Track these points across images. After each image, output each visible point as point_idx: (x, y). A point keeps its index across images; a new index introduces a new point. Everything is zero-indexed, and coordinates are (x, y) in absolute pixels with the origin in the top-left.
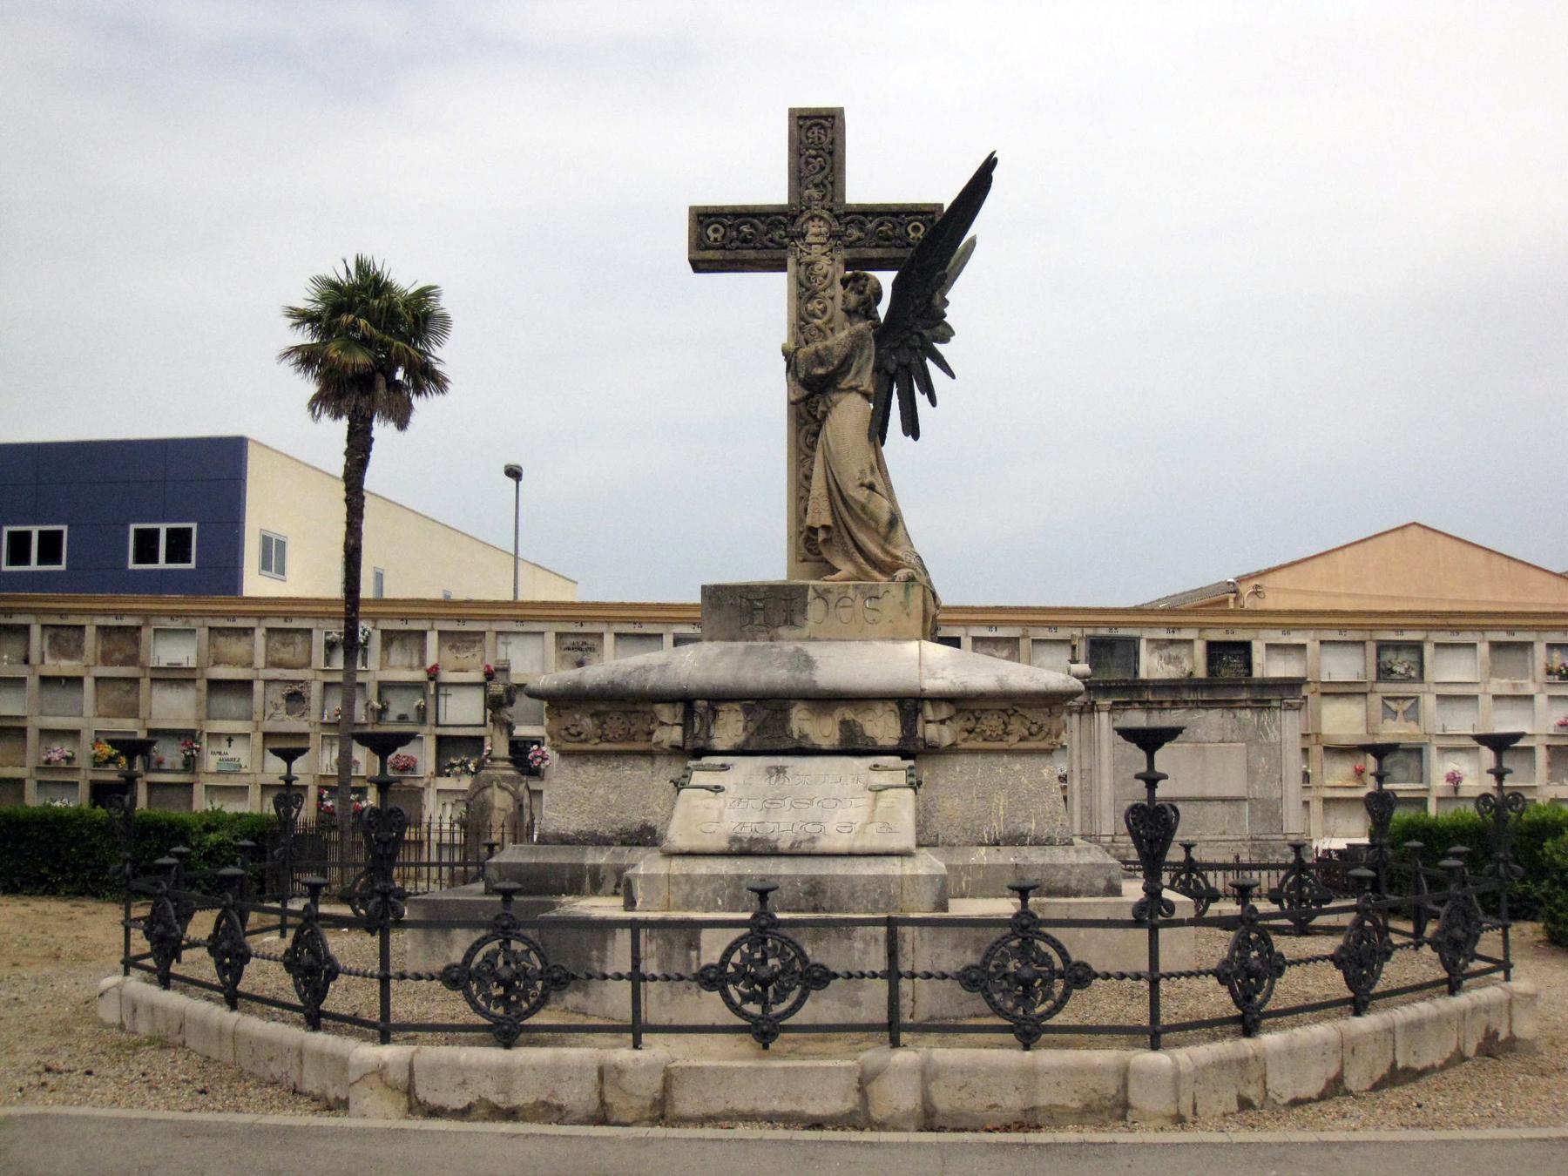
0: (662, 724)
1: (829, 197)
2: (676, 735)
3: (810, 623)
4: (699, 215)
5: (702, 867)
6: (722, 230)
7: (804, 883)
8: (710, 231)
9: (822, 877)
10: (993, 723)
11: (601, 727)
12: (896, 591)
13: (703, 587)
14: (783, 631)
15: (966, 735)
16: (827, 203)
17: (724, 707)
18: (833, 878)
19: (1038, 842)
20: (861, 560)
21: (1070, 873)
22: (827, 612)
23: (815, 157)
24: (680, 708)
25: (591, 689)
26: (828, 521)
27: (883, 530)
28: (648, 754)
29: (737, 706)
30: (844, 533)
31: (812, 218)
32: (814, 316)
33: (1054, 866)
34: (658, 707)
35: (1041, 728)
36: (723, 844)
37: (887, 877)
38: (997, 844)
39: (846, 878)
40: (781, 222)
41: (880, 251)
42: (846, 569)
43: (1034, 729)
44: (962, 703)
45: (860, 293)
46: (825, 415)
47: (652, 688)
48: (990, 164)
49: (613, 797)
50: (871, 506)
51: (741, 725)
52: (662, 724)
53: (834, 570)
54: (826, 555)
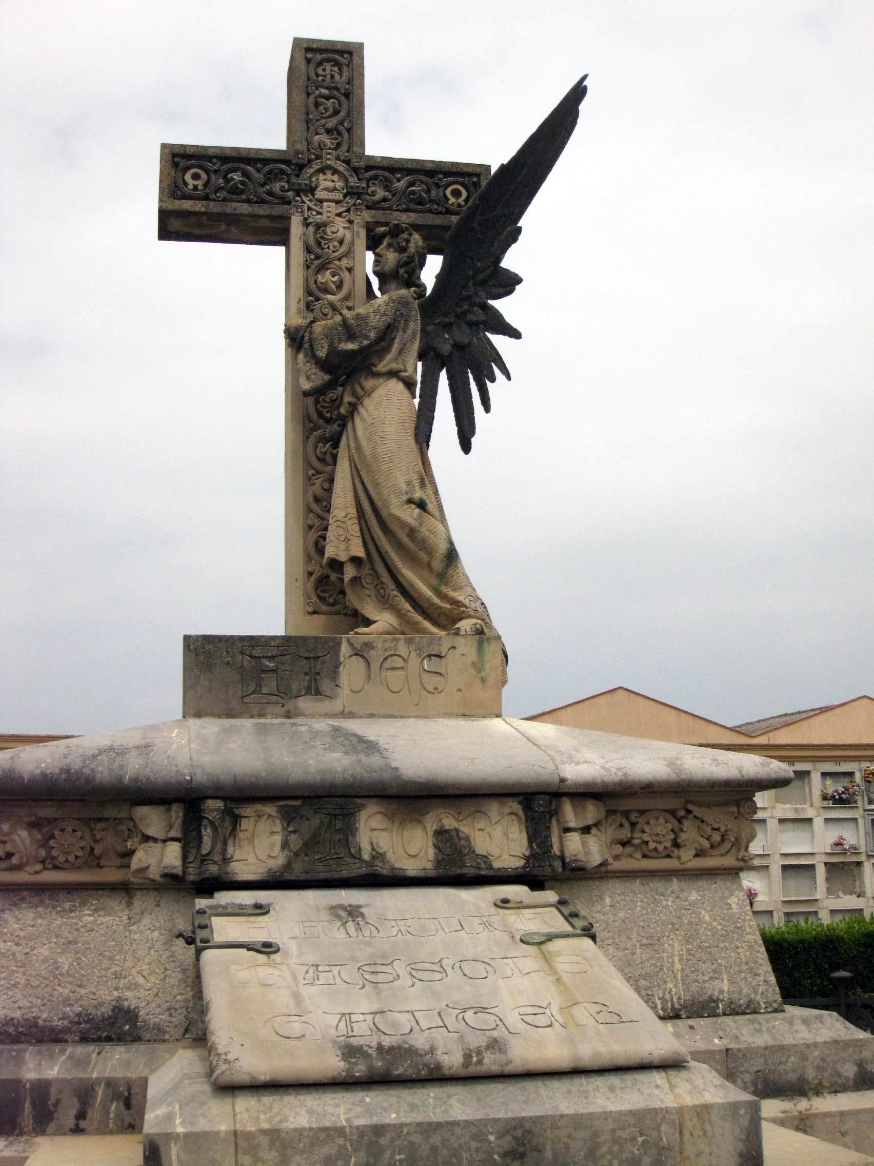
0: (147, 838)
1: (344, 147)
2: (172, 856)
3: (344, 692)
4: (174, 155)
5: (299, 1113)
6: (204, 176)
7: (500, 1136)
8: (188, 177)
9: (536, 1120)
10: (659, 830)
11: (44, 844)
12: (466, 648)
13: (187, 638)
14: (305, 703)
15: (619, 849)
16: (342, 152)
17: (248, 811)
18: (555, 1121)
19: (734, 1010)
20: (407, 606)
21: (804, 1058)
22: (368, 677)
23: (327, 98)
24: (177, 813)
25: (33, 780)
26: (360, 552)
27: (437, 565)
28: (124, 889)
29: (270, 809)
30: (373, 573)
31: (322, 171)
32: (327, 291)
33: (782, 1048)
34: (142, 811)
35: (723, 838)
36: (333, 1064)
37: (655, 1111)
38: (677, 1016)
39: (577, 1121)
40: (282, 172)
41: (412, 215)
42: (384, 620)
43: (717, 837)
44: (615, 800)
45: (402, 250)
46: (353, 408)
47: (135, 780)
48: (578, 93)
49: (65, 961)
50: (424, 531)
51: (278, 839)
52: (147, 838)
53: (368, 622)
54: (353, 599)
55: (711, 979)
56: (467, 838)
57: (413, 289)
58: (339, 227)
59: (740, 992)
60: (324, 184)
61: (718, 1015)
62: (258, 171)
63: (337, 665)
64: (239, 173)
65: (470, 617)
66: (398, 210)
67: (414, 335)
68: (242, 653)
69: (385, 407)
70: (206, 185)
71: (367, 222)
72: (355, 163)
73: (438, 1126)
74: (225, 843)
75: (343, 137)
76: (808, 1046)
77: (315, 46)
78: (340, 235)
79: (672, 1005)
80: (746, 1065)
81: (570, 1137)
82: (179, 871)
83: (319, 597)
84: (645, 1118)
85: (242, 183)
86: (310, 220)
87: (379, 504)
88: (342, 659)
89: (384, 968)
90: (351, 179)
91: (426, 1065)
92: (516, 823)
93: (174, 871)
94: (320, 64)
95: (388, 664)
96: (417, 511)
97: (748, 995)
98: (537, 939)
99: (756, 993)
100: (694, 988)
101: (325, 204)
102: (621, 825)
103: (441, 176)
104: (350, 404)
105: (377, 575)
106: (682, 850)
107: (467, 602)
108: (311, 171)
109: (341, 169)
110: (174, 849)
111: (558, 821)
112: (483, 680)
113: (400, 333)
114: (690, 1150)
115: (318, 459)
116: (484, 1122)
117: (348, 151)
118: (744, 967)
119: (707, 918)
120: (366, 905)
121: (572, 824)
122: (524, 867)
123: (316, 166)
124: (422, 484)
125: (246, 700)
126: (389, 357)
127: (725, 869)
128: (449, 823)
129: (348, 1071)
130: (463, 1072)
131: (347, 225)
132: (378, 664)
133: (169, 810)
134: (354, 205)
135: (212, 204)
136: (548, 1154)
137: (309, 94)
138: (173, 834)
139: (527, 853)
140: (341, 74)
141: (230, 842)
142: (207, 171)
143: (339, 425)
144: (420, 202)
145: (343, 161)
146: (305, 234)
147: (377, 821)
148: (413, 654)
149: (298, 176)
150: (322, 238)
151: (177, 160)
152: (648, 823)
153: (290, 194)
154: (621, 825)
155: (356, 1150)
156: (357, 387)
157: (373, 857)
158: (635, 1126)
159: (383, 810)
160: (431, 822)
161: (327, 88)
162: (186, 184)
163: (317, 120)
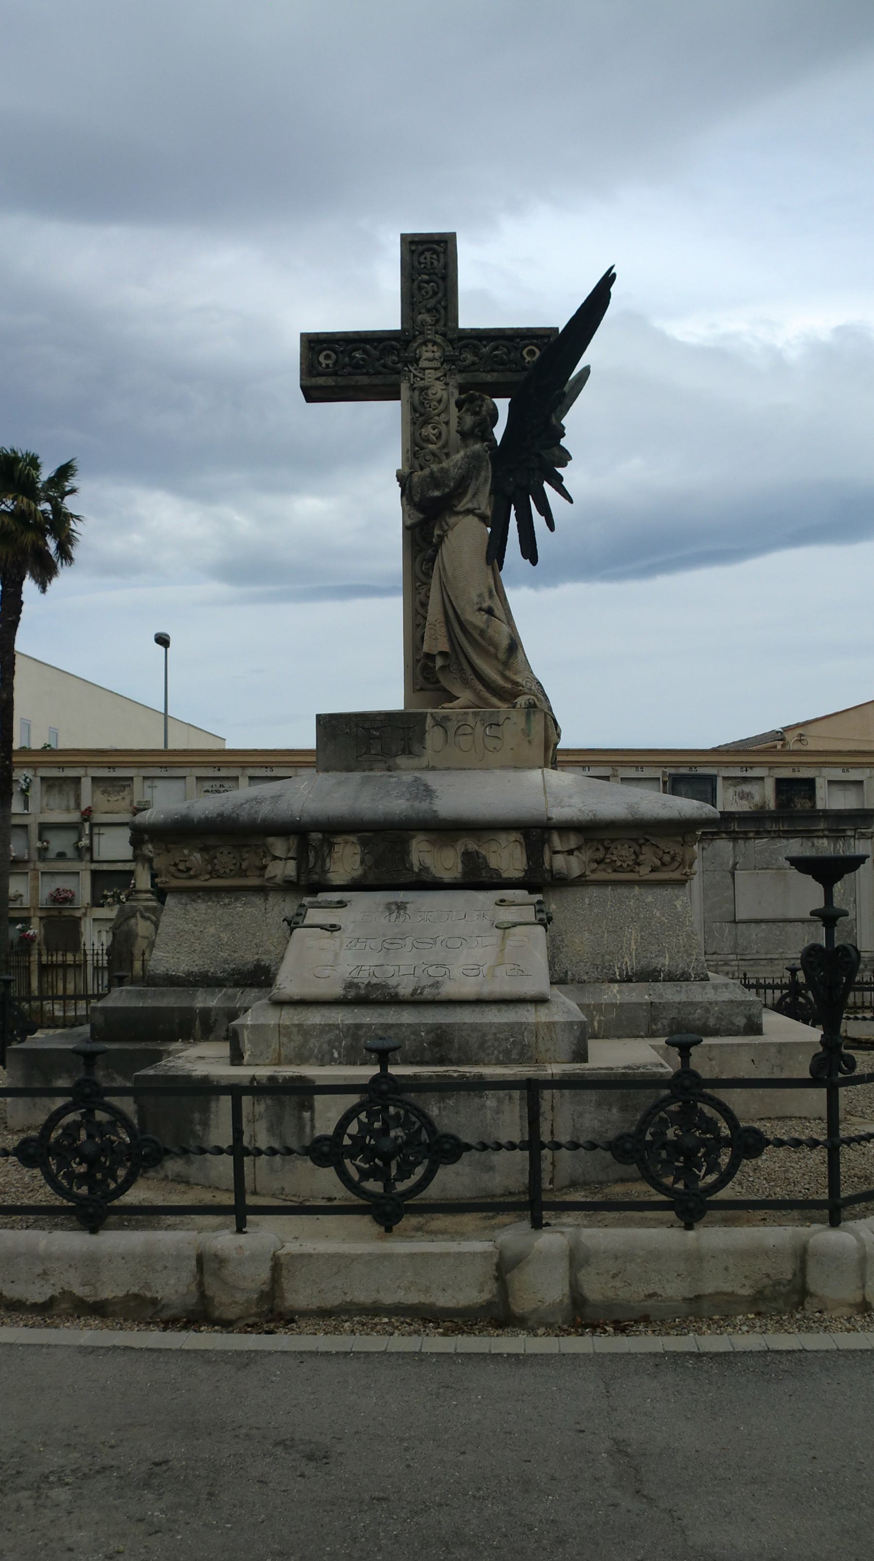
0: (275, 858)
1: (442, 323)
2: (289, 869)
3: (429, 752)
4: (310, 342)
5: (315, 1017)
6: (333, 356)
7: (428, 1033)
8: (321, 358)
9: (449, 1025)
10: (624, 853)
11: (211, 861)
12: (517, 718)
13: (318, 716)
14: (401, 761)
15: (595, 865)
16: (440, 328)
17: (339, 839)
18: (461, 1026)
19: (671, 978)
20: (480, 687)
21: (707, 1010)
22: (446, 741)
23: (428, 282)
24: (293, 841)
25: (200, 821)
26: (446, 648)
27: (502, 656)
28: (262, 891)
29: (353, 838)
31: (425, 343)
32: (428, 440)
33: (691, 1003)
34: (271, 840)
35: (673, 858)
36: (338, 991)
37: (522, 1024)
38: (630, 980)
39: (474, 1027)
40: (393, 348)
41: (495, 374)
42: (465, 696)
43: (667, 858)
44: (591, 832)
45: (476, 414)
46: (441, 538)
47: (264, 820)
48: (608, 279)
49: (225, 936)
50: (490, 632)
51: (358, 858)
52: (275, 858)
53: (453, 698)
54: (444, 683)
55: (657, 956)
56: (484, 858)
57: (486, 443)
58: (438, 390)
59: (677, 966)
60: (426, 355)
61: (660, 981)
62: (375, 348)
63: (424, 732)
64: (361, 352)
65: (525, 693)
66: (484, 371)
67: (486, 480)
68: (357, 726)
69: (465, 536)
70: (335, 364)
71: (459, 384)
72: (450, 336)
73: (392, 1025)
74: (324, 861)
75: (440, 314)
76: (711, 1003)
77: (417, 239)
78: (438, 396)
79: (627, 973)
80: (665, 1014)
81: (469, 1035)
82: (294, 879)
83: (425, 678)
84: (516, 1028)
85: (363, 359)
86: (415, 386)
87: (459, 612)
88: (427, 728)
89: (400, 941)
90: (447, 349)
91: (389, 994)
92: (519, 847)
93: (291, 879)
94: (422, 253)
95: (460, 732)
96: (486, 616)
97: (683, 968)
98: (506, 925)
99: (689, 967)
100: (643, 962)
101: (427, 371)
102: (598, 849)
103: (518, 340)
104: (438, 535)
105: (460, 664)
106: (642, 867)
107: (524, 683)
108: (416, 345)
109: (439, 341)
110: (292, 864)
111: (550, 847)
112: (530, 742)
113: (474, 481)
114: (542, 1048)
115: (423, 573)
116: (419, 1025)
117: (445, 325)
118: (682, 949)
119: (658, 914)
120: (412, 902)
121: (559, 848)
122: (524, 877)
123: (420, 341)
124: (491, 595)
125: (360, 759)
126: (465, 500)
127: (673, 881)
128: (472, 846)
129: (344, 995)
130: (412, 999)
131: (444, 387)
132: (453, 732)
133: (288, 839)
134: (450, 370)
135: (339, 379)
136: (456, 1045)
137: (413, 281)
138: (290, 855)
139: (526, 868)
140: (438, 261)
141: (328, 860)
142: (336, 352)
143: (433, 551)
144: (503, 363)
145: (441, 335)
146: (411, 397)
147: (425, 846)
148: (479, 724)
149: (406, 350)
150: (425, 399)
151: (313, 345)
152: (616, 848)
153: (399, 365)
154: (598, 849)
155: (345, 1037)
156: (443, 523)
157: (420, 870)
158: (508, 1031)
159: (427, 838)
160: (460, 847)
161: (426, 274)
162: (320, 364)
163: (420, 302)
